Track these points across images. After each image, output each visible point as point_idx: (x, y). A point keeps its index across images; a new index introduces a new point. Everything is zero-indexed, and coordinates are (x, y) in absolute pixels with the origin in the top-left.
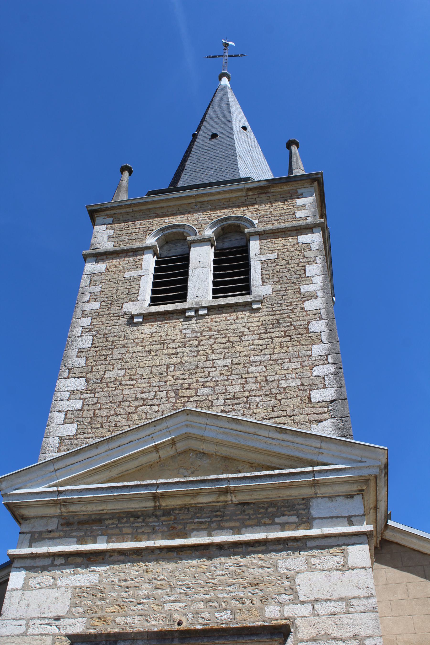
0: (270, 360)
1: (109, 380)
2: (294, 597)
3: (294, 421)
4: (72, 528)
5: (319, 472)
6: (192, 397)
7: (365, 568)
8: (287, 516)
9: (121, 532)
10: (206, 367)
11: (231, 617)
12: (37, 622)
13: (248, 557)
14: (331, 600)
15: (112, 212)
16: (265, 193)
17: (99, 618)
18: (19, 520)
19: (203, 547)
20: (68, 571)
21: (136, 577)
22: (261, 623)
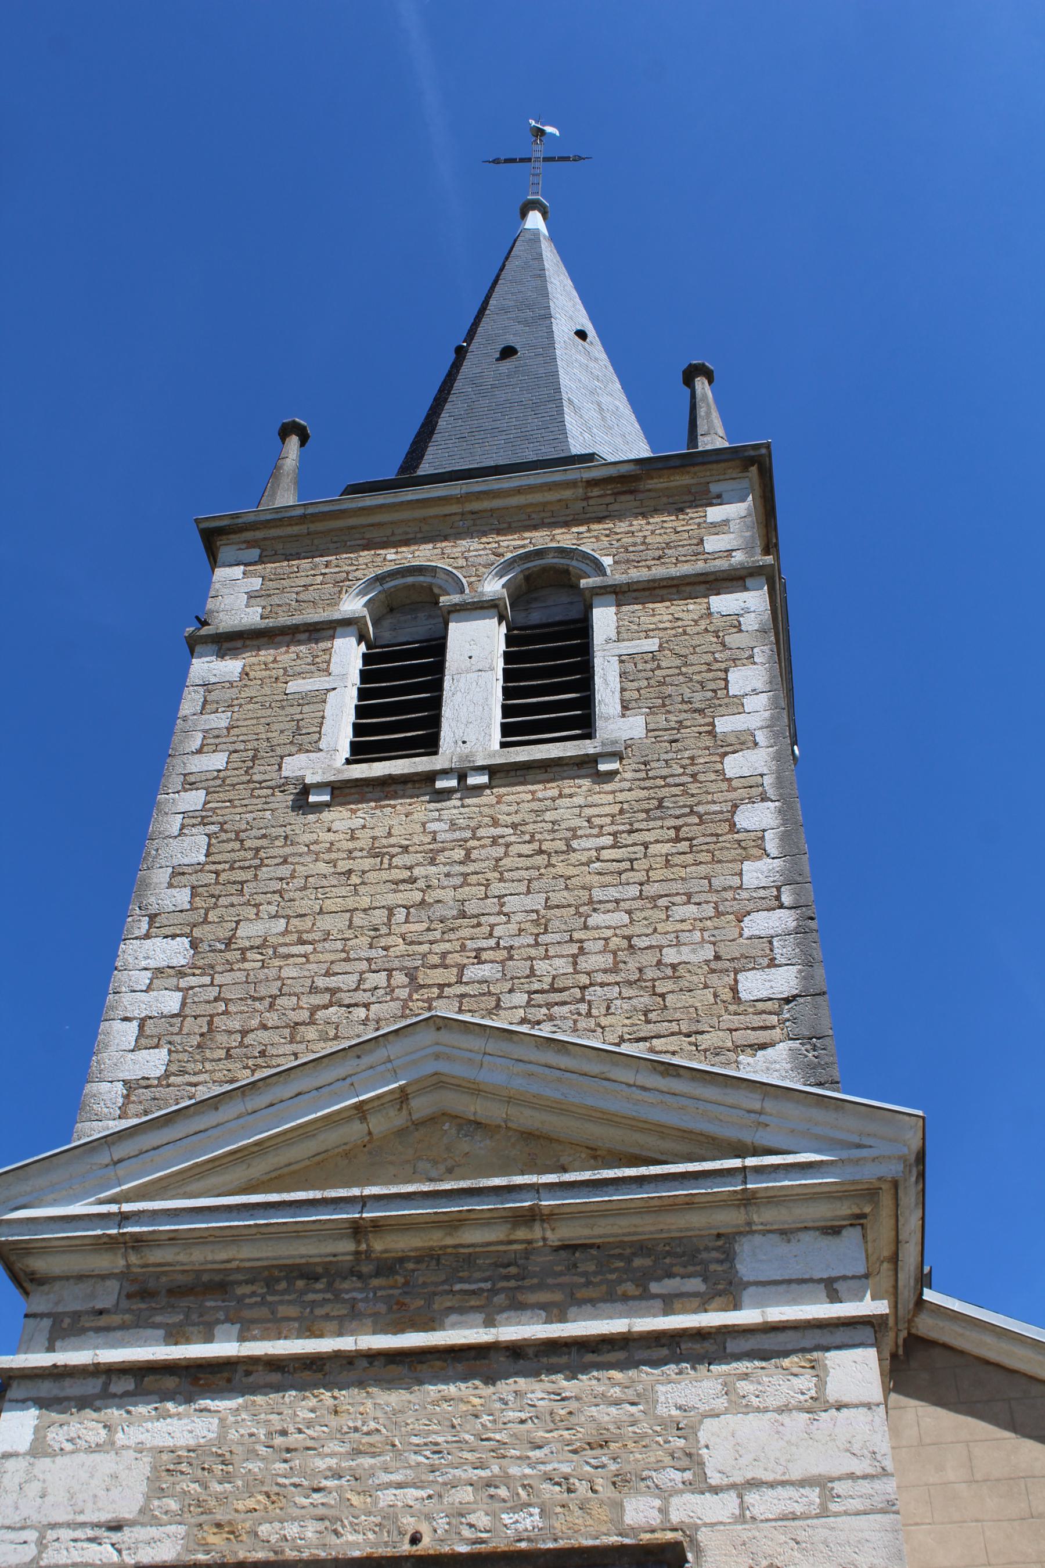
0: (641, 897)
1: (247, 944)
2: (694, 1474)
3: (696, 1046)
4: (153, 1305)
5: (758, 1170)
6: (449, 985)
7: (868, 1406)
8: (678, 1279)
9: (272, 1313)
10: (483, 915)
11: (540, 1525)
12: (66, 1534)
13: (584, 1377)
14: (783, 1483)
15: (259, 534)
16: (631, 492)
17: (219, 1525)
18: (25, 1285)
19: (473, 1353)
20: (142, 1409)
21: (310, 1424)
22: (614, 1539)
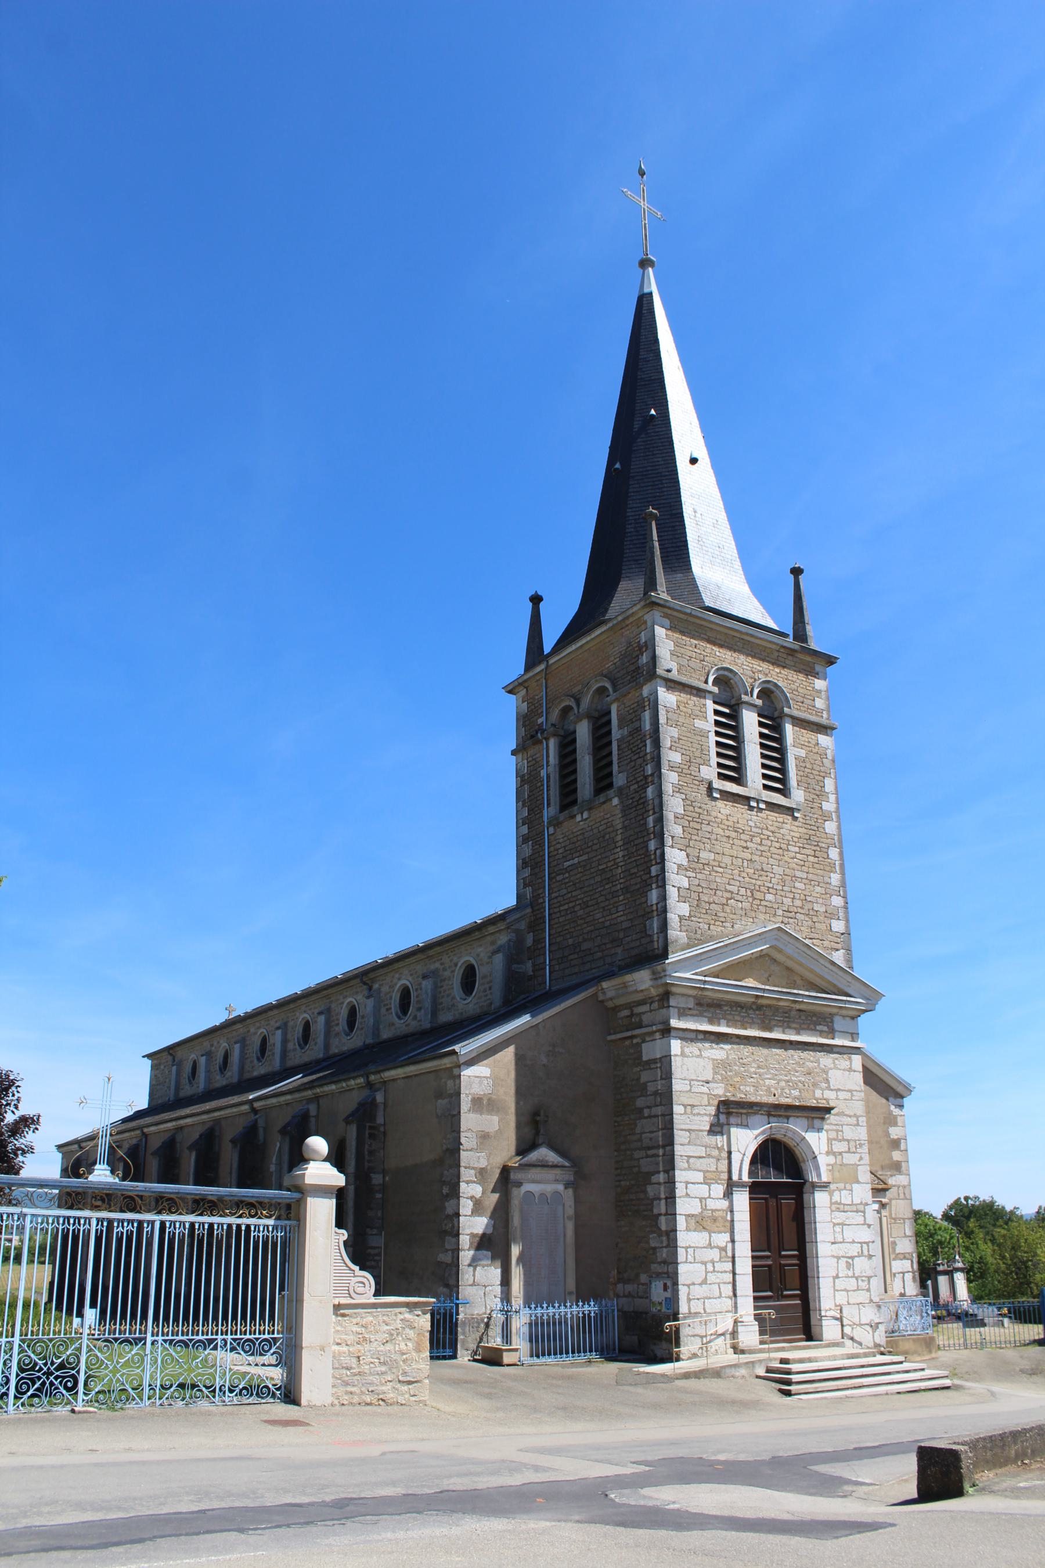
1: (704, 862)
5: (849, 1001)
15: (669, 612)
21: (748, 1057)
